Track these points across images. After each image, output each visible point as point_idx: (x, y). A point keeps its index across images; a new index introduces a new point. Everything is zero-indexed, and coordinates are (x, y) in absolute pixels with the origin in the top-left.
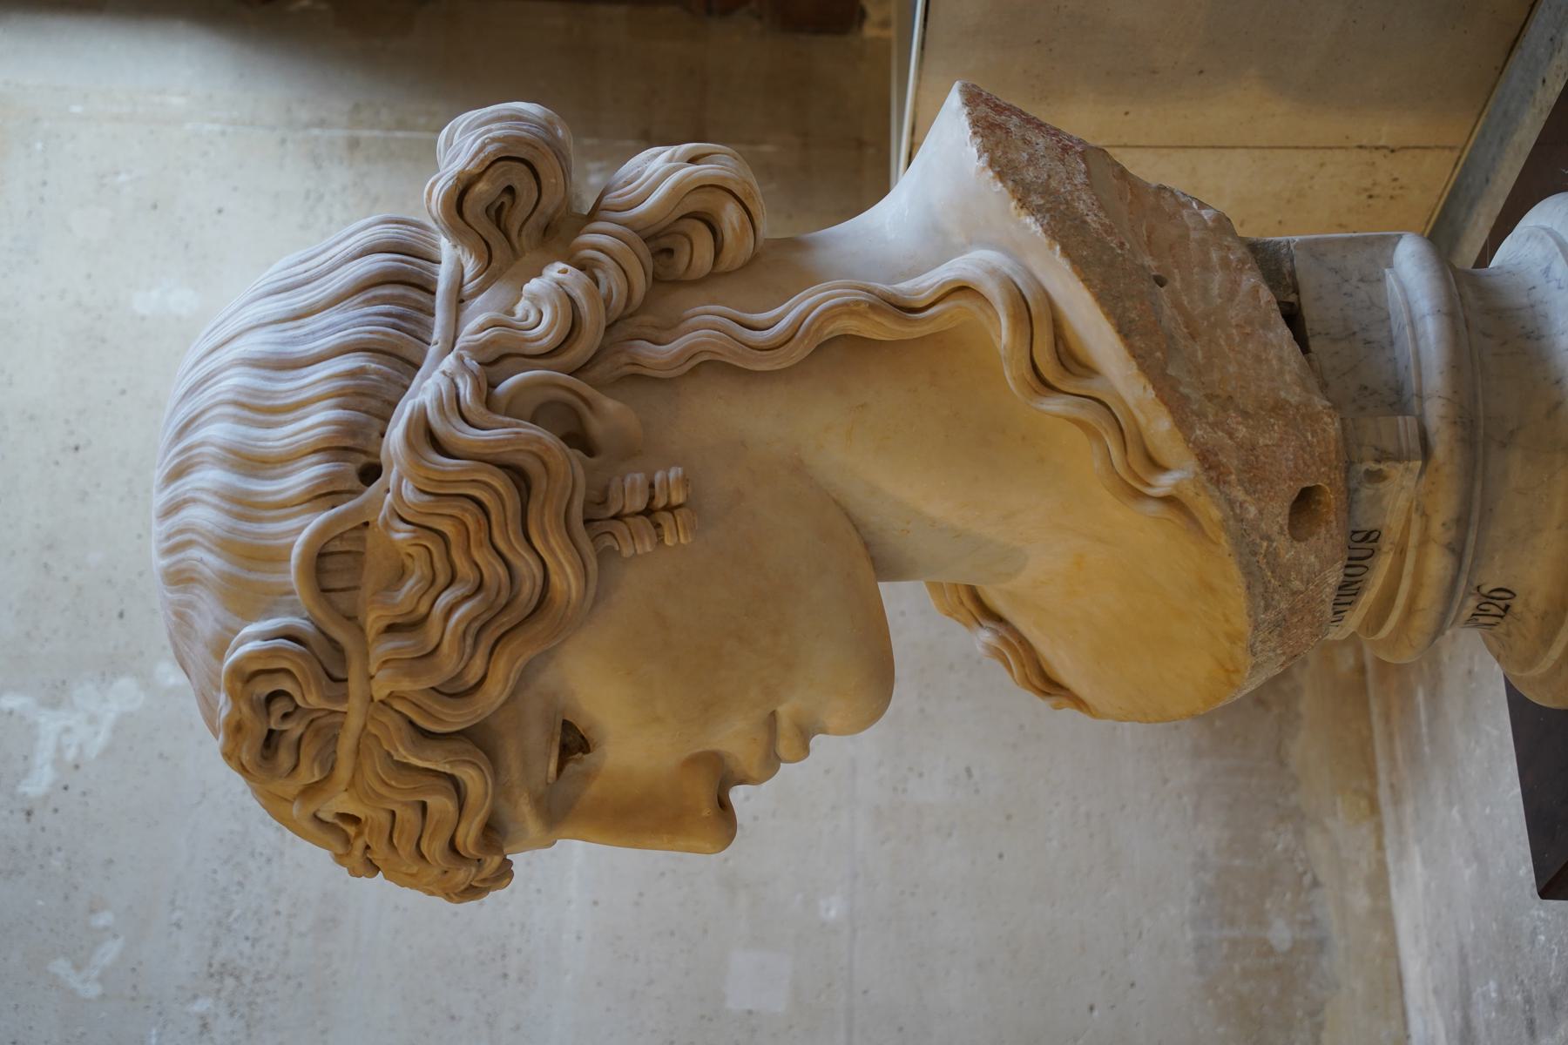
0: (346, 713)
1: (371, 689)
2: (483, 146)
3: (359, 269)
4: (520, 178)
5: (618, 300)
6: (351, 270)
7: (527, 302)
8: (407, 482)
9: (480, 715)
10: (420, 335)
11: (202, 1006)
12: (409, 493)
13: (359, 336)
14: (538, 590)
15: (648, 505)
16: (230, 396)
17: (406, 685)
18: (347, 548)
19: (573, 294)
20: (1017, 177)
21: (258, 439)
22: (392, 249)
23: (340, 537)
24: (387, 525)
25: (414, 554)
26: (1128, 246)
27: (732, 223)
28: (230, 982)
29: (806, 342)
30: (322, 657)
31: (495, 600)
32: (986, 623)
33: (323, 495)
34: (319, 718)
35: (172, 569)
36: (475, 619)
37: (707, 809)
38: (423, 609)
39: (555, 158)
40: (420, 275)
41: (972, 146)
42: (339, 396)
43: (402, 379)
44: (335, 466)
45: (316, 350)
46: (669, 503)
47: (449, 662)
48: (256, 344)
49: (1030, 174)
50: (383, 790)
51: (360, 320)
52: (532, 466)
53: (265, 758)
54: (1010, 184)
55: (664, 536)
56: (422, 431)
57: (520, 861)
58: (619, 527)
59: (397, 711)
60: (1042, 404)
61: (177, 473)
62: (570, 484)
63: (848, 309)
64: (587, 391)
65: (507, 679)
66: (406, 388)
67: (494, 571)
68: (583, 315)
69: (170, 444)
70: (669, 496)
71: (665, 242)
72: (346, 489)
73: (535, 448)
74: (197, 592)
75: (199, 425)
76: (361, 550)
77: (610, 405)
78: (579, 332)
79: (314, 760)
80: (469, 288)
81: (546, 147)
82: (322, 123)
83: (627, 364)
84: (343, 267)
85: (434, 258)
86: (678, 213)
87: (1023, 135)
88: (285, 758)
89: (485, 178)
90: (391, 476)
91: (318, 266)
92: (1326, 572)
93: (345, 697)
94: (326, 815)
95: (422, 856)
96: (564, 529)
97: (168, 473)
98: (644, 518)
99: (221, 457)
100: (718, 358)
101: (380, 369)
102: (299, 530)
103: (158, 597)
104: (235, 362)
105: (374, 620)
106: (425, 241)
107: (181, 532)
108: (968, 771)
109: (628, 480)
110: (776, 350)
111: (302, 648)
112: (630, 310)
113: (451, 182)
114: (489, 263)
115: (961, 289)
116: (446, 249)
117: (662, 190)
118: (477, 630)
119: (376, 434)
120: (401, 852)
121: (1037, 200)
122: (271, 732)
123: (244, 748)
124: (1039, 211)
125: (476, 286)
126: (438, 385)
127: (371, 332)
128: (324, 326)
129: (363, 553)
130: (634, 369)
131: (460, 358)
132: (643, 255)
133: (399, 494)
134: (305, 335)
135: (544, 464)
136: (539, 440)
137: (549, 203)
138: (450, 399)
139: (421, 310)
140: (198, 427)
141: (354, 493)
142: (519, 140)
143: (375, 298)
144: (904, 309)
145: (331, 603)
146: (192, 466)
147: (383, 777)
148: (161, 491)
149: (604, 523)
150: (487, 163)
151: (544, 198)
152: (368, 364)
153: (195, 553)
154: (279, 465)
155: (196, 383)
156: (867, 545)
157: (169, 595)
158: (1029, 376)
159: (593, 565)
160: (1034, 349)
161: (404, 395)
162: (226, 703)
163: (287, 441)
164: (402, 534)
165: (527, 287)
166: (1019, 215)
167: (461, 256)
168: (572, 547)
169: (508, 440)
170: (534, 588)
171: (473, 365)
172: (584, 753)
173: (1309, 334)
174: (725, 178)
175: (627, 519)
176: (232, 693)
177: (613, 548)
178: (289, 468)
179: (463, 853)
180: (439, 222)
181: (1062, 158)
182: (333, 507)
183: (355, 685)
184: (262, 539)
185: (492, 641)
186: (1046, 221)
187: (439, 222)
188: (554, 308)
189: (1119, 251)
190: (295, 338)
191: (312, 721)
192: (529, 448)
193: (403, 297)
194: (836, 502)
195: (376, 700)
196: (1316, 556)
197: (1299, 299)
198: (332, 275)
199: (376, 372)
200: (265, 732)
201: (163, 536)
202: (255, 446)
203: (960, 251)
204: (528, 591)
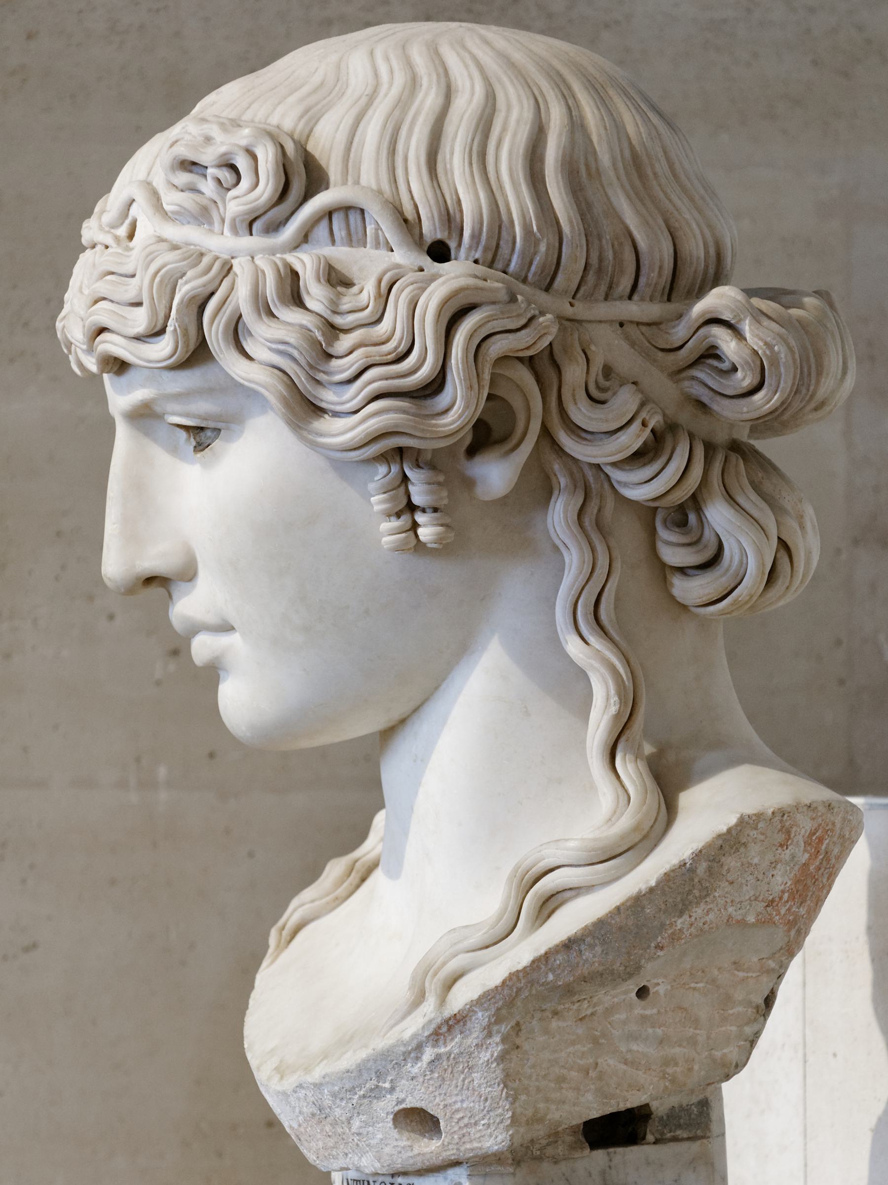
0: (222, 234)
26: (660, 953)
34: (217, 207)
46: (419, 525)
55: (390, 521)
76: (368, 245)
88: (183, 178)
92: (370, 1153)
95: (96, 302)
129: (365, 247)
151: (726, 402)
172: (195, 447)
173: (611, 1150)
179: (99, 339)
181: (760, 898)
189: (653, 945)
191: (215, 202)
195: (233, 261)
196: (382, 1140)
197: (648, 1144)
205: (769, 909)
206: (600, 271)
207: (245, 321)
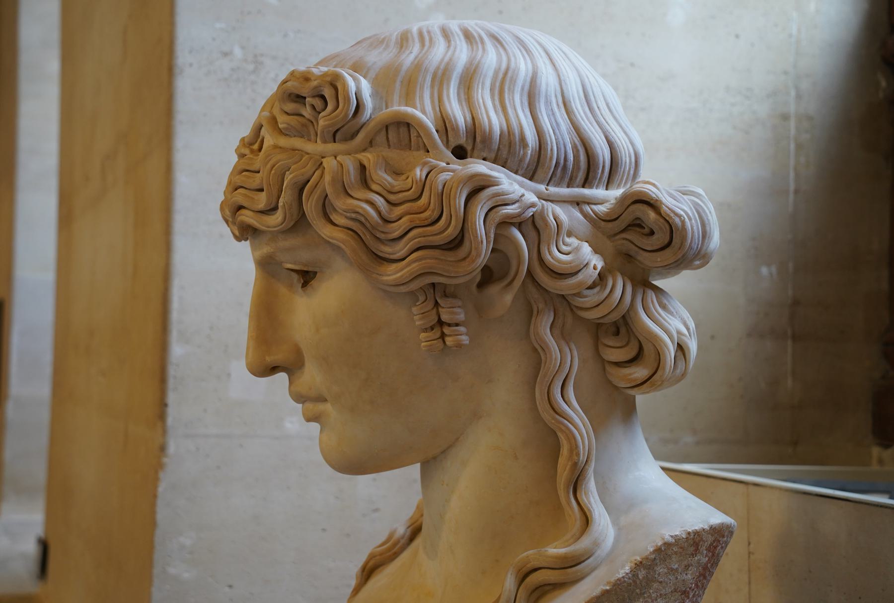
0: (316, 142)
1: (328, 156)
2: (679, 216)
3: (597, 140)
4: (659, 239)
5: (578, 302)
6: (597, 135)
7: (577, 244)
8: (451, 175)
9: (312, 222)
10: (553, 179)
11: (238, 52)
12: (444, 177)
13: (549, 143)
14: (387, 256)
15: (446, 323)
16: (513, 65)
17: (327, 178)
18: (412, 140)
19: (580, 274)
20: (658, 561)
21: (483, 84)
22: (613, 159)
23: (419, 136)
24: (425, 164)
25: (408, 180)
27: (634, 373)
28: (251, 67)
29: (553, 421)
30: (346, 127)
31: (378, 230)
32: (409, 530)
33: (445, 126)
34: (314, 126)
35: (409, 35)
36: (366, 219)
37: (270, 359)
38: (374, 187)
39: (675, 260)
40: (595, 178)
41: (680, 531)
42: (509, 132)
43: (522, 169)
44: (463, 130)
45: (540, 117)
47: (341, 203)
48: (548, 80)
49: (661, 569)
50: (269, 166)
51: (562, 142)
52: (463, 252)
53: (290, 95)
54: (653, 556)
55: (426, 332)
56: (482, 184)
57: (245, 247)
58: (430, 304)
59: (315, 172)
60: (511, 574)
61: (468, 36)
62: (452, 275)
63: (574, 448)
64: (518, 283)
65: (332, 238)
66: (516, 173)
67: (397, 229)
68: (566, 280)
69: (488, 31)
70: (450, 336)
71: (623, 330)
72: (449, 139)
73: (474, 253)
74: (394, 51)
75: (497, 47)
76: (412, 149)
77: (509, 298)
78: (556, 278)
79: (288, 124)
80: (587, 208)
81: (681, 255)
82: (799, 97)
83: (538, 308)
84: (600, 130)
85: (610, 186)
86: (641, 339)
87: (692, 565)
88: (290, 107)
89: (658, 217)
90: (457, 166)
91: (602, 115)
93: (325, 142)
94: (263, 132)
95: (236, 189)
96: (422, 272)
97: (469, 31)
98: (436, 320)
99: (473, 62)
100: (543, 365)
101: (527, 156)
102: (424, 112)
103: (394, 29)
104: (536, 68)
105: (368, 158)
106: (622, 180)
107: (431, 40)
108: (376, 510)
109: (459, 310)
110: (548, 402)
111: (351, 116)
112: (574, 309)
113: (654, 196)
114: (604, 221)
115: (587, 520)
116: (615, 193)
117: (654, 328)
118: (359, 219)
119: (485, 155)
120: (237, 177)
121: (642, 574)
122: (305, 98)
123: (295, 83)
124: (633, 575)
125: (588, 213)
126: (514, 193)
127: (552, 150)
128: (558, 121)
130: (535, 312)
131: (533, 205)
132: (610, 316)
133: (444, 170)
134: (552, 109)
135: (465, 259)
136: (479, 255)
137: (646, 259)
138: (504, 200)
139: (571, 179)
140: (496, 47)
141: (447, 143)
142: (684, 238)
143: (578, 151)
144: (576, 484)
145: (380, 131)
146: (471, 44)
147: (277, 166)
148: (459, 26)
149: (432, 295)
150: (667, 219)
152: (530, 149)
153: (416, 48)
154: (466, 97)
155: (525, 44)
156: (435, 458)
157: (396, 33)
158: (530, 566)
159: (403, 289)
160: (546, 570)
161: (511, 172)
162: (321, 71)
163: (481, 101)
164: (419, 173)
165: (586, 244)
166: (631, 562)
167: (609, 203)
168: (413, 276)
169: (477, 237)
170: (388, 254)
171: (530, 213)
172: (303, 284)
174: (664, 368)
175: (435, 310)
176: (325, 74)
177: (418, 300)
178: (464, 103)
179: (238, 213)
180: (630, 189)
181: (678, 591)
182: (437, 131)
183: (331, 147)
184: (420, 88)
185: (354, 229)
186: (626, 580)
187: (630, 189)
188: (570, 262)
190: (550, 103)
191: (312, 122)
192: (473, 250)
193: (579, 168)
194: (457, 439)
195: (323, 160)
198: (595, 124)
199: (525, 154)
200: (304, 95)
201: (430, 28)
202: (479, 83)
203: (615, 523)
204: (387, 250)
205: (683, 596)
206: (565, 167)
207: (330, 198)
